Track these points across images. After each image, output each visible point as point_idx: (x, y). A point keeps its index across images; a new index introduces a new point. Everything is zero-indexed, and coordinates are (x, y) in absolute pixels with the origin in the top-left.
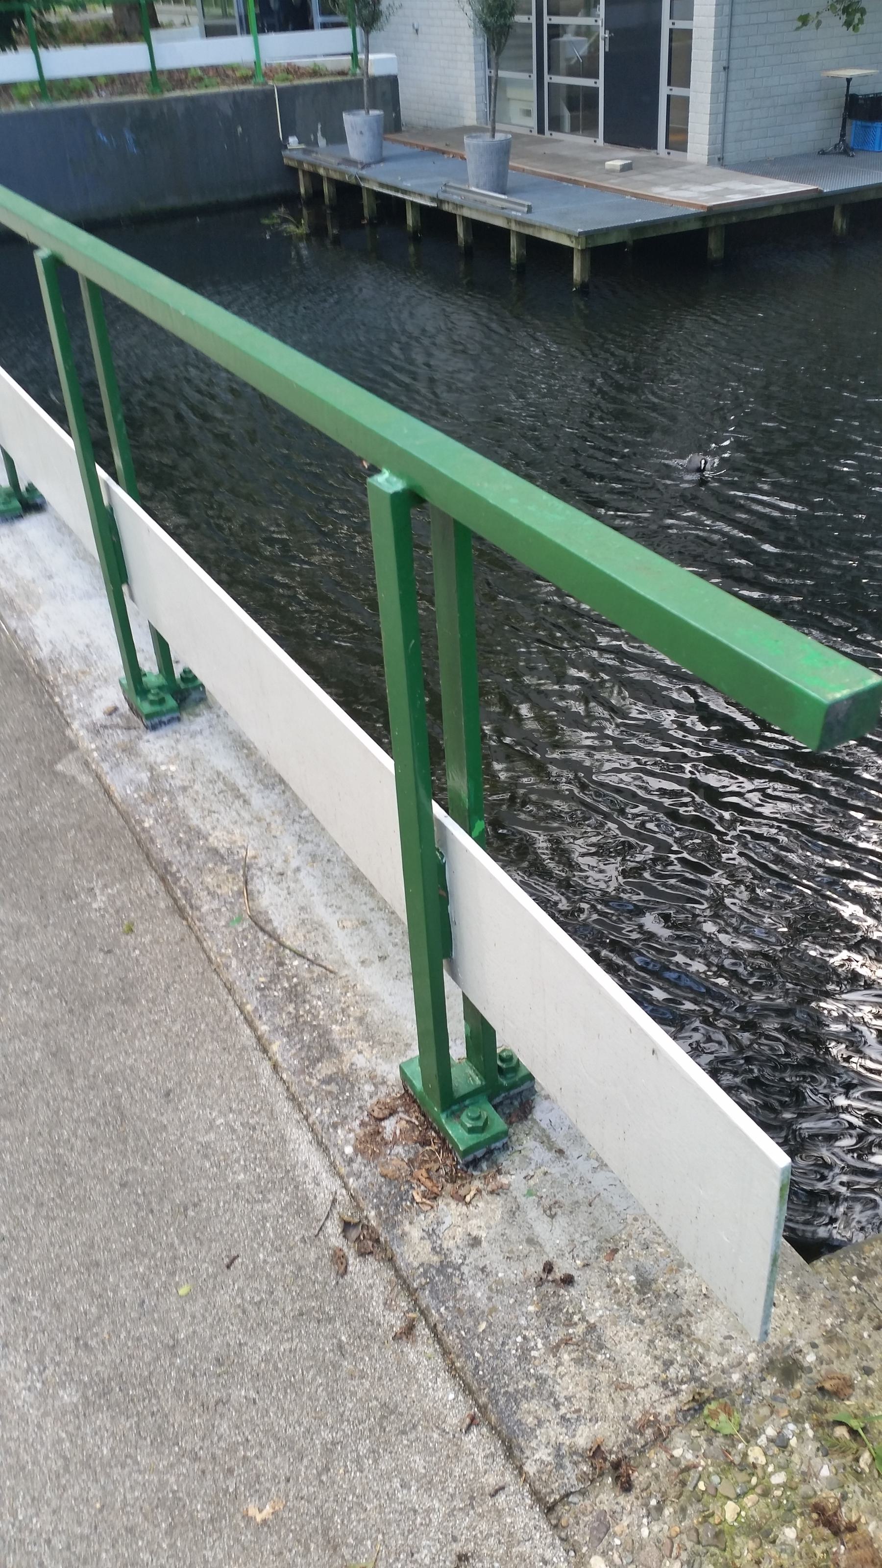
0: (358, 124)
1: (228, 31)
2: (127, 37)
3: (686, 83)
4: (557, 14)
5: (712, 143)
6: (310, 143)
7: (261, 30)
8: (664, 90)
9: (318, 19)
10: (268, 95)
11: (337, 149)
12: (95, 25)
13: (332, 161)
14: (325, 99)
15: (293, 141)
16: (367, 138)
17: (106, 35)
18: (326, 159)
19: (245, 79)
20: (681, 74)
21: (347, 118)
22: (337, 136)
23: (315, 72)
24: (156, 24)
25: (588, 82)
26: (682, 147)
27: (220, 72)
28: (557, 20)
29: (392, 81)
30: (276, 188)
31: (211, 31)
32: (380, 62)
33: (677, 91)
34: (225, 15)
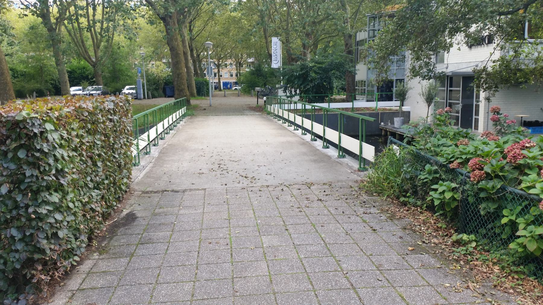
0: (397, 121)
1: (373, 101)
2: (348, 101)
3: (478, 116)
4: (451, 100)
5: (484, 128)
6: (386, 124)
7: (379, 101)
8: (474, 117)
9: (394, 99)
10: (337, 115)
11: (393, 126)
12: (341, 99)
13: (390, 128)
14: (391, 115)
15: (382, 124)
16: (399, 123)
17: (343, 101)
18: (389, 126)
19: (373, 110)
20: (477, 114)
21: (395, 119)
22: (393, 123)
23: (390, 110)
24: (355, 99)
25: (457, 115)
26: (477, 129)
27: (367, 109)
28: (450, 101)
29: (409, 112)
30: (377, 133)
31: (368, 101)
32: (405, 108)
33: (477, 117)
34: (372, 98)
